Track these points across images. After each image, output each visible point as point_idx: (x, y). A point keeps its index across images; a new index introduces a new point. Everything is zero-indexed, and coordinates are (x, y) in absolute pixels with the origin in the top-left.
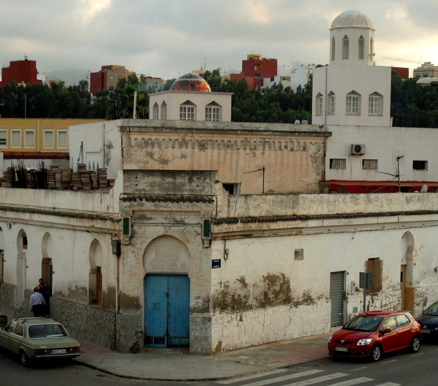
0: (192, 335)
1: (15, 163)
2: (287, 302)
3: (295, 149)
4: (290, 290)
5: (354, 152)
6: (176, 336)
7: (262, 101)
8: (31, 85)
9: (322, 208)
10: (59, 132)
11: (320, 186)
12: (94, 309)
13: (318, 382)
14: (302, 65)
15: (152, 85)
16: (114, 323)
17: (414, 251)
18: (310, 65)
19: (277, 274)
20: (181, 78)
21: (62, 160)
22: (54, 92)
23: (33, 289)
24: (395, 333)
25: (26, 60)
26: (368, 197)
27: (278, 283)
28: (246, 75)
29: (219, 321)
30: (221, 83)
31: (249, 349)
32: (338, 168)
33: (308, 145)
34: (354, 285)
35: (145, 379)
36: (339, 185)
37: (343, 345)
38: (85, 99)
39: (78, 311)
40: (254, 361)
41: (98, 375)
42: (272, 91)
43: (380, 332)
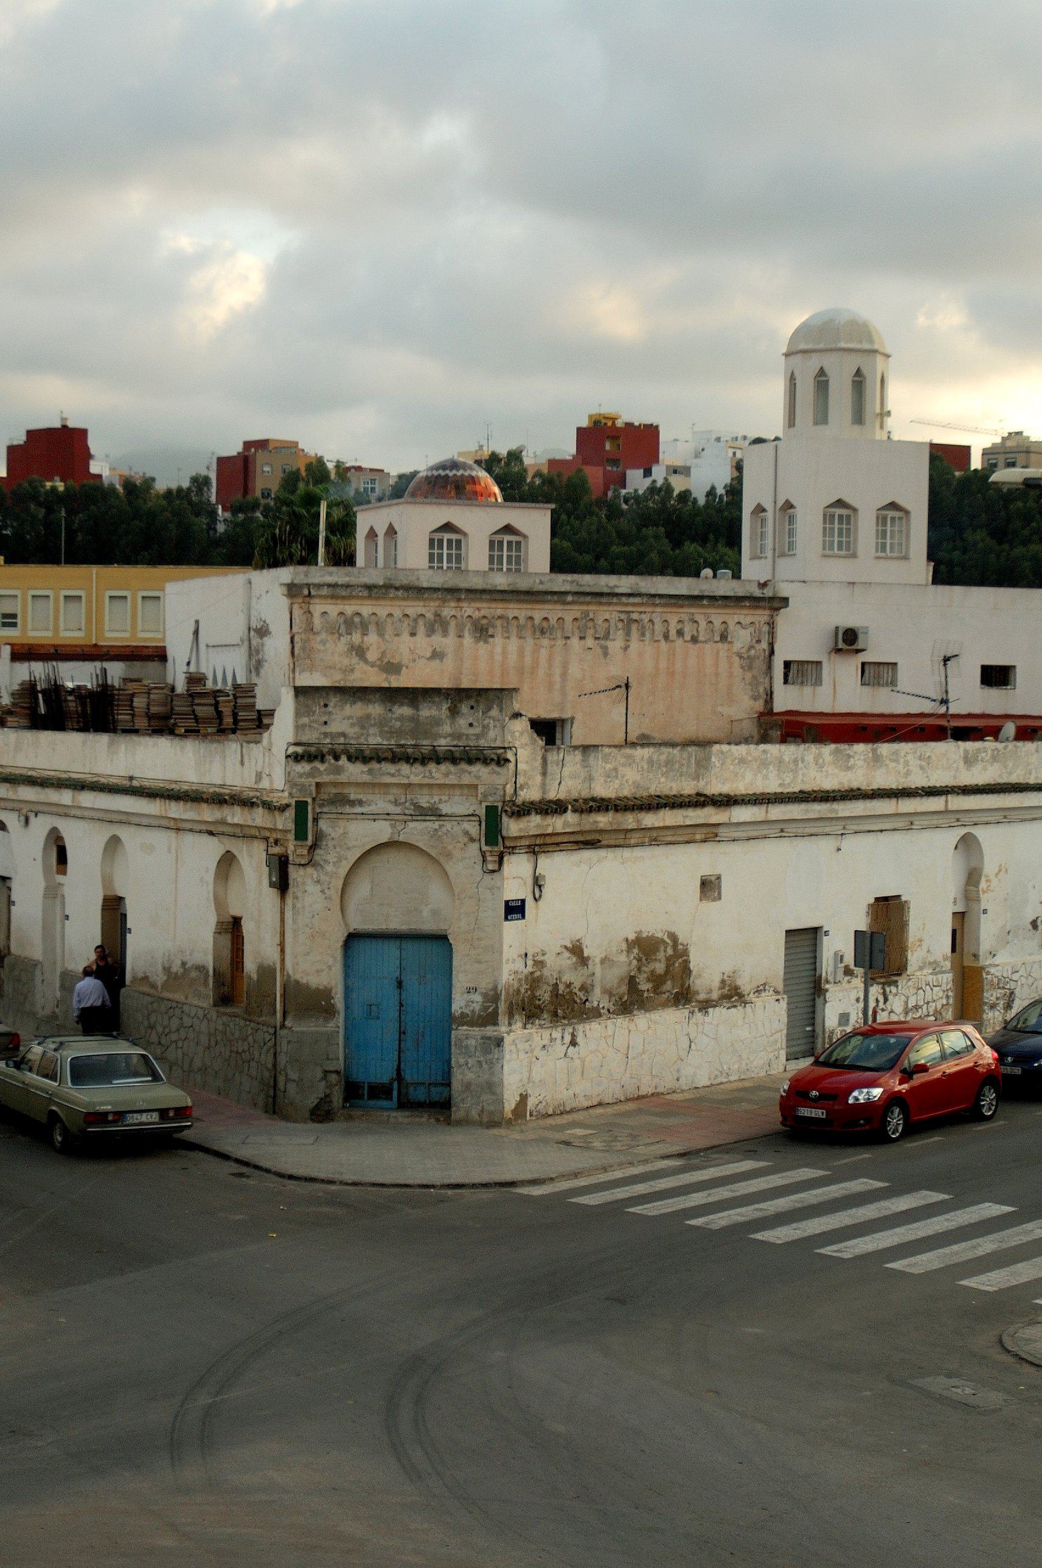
0: (458, 1078)
1: (38, 670)
2: (683, 1002)
3: (701, 638)
4: (691, 971)
5: (841, 645)
6: (421, 1080)
7: (623, 523)
8: (77, 486)
9: (766, 778)
10: (143, 598)
11: (760, 725)
12: (225, 1019)
13: (755, 1190)
14: (718, 439)
15: (362, 485)
16: (272, 1051)
17: (983, 879)
18: (736, 439)
19: (660, 935)
20: (432, 469)
21: (150, 664)
22: (130, 503)
23: (81, 970)
24: (939, 1075)
25: (64, 427)
26: (874, 751)
27: (661, 955)
28: (586, 461)
29: (521, 1046)
30: (525, 480)
31: (591, 1111)
32: (802, 683)
33: (731, 627)
34: (841, 961)
35: (347, 1184)
36: (803, 724)
37: (814, 1103)
38: (204, 520)
39: (187, 1021)
40: (604, 1141)
41: (234, 1175)
42: (647, 500)
43: (904, 1071)
